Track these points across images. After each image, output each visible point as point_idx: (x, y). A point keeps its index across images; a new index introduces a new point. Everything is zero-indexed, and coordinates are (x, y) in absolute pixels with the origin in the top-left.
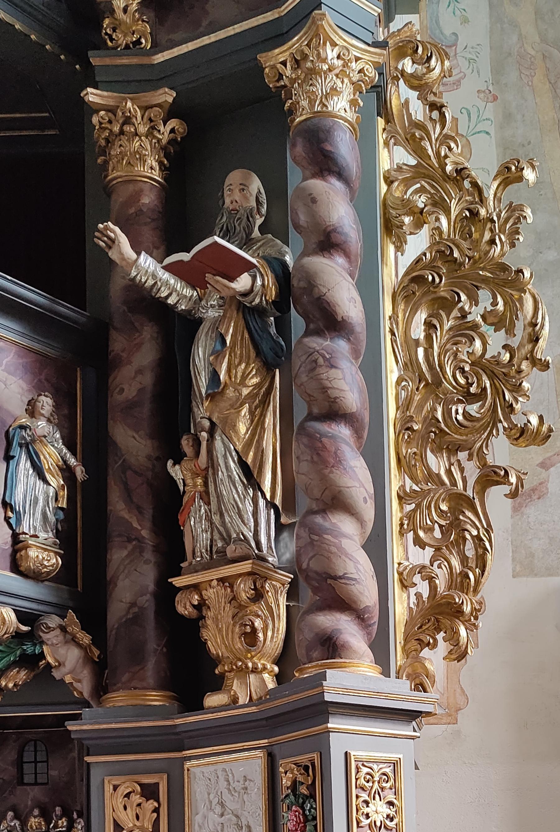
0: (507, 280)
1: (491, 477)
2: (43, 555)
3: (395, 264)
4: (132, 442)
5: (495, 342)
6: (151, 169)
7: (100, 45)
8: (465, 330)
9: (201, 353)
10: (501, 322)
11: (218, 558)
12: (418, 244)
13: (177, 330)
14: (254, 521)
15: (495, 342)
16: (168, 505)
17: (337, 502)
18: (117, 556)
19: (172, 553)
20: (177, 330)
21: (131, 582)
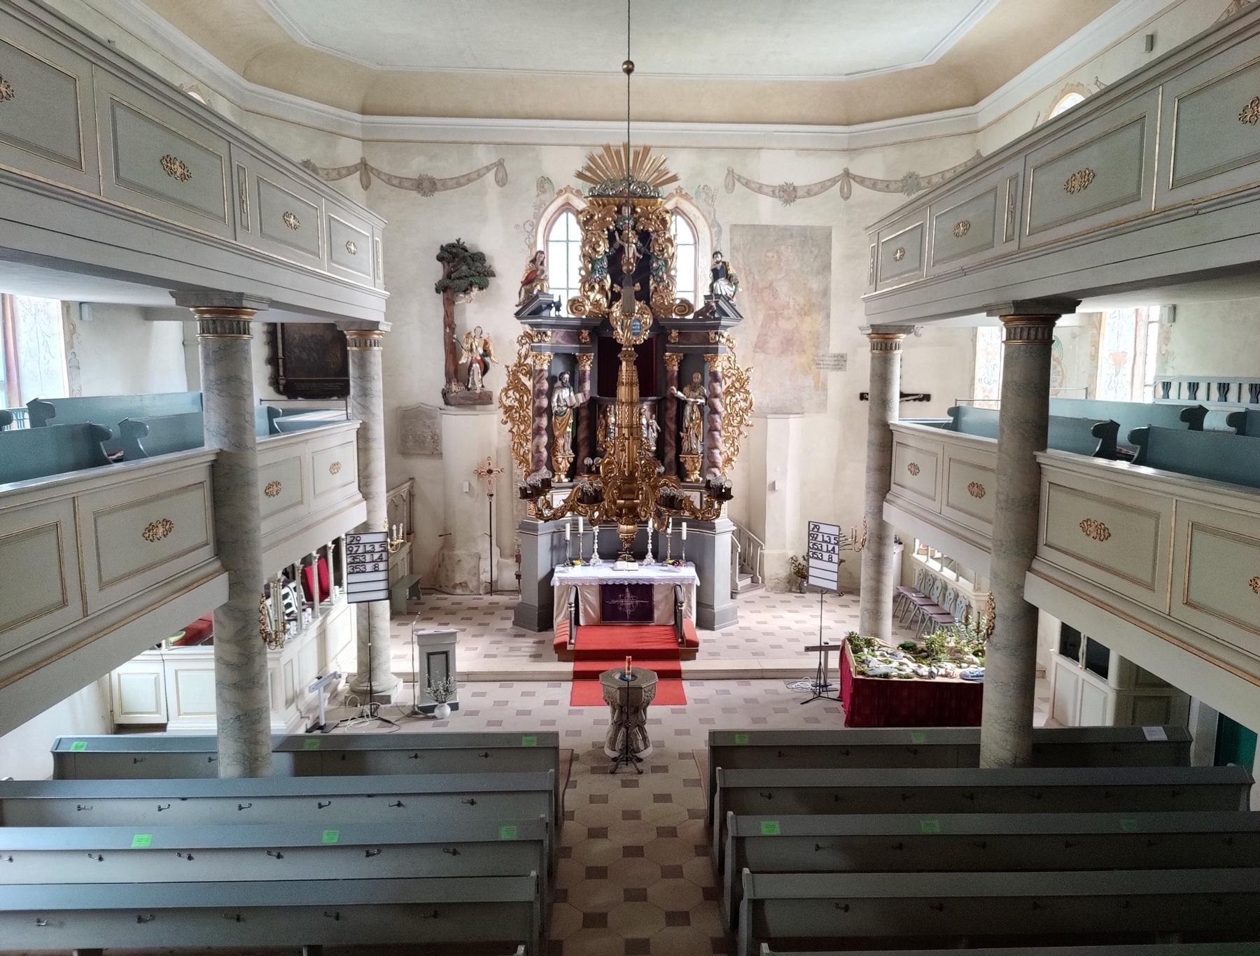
0: (747, 392)
1: (741, 433)
2: (654, 448)
3: (724, 387)
4: (672, 426)
5: (743, 404)
6: (676, 368)
7: (669, 342)
8: (736, 402)
9: (688, 409)
10: (745, 400)
11: (690, 453)
12: (729, 382)
13: (682, 404)
14: (698, 446)
15: (743, 404)
16: (679, 441)
17: (716, 447)
18: (667, 449)
19: (679, 449)
20: (682, 404)
21: (671, 454)
